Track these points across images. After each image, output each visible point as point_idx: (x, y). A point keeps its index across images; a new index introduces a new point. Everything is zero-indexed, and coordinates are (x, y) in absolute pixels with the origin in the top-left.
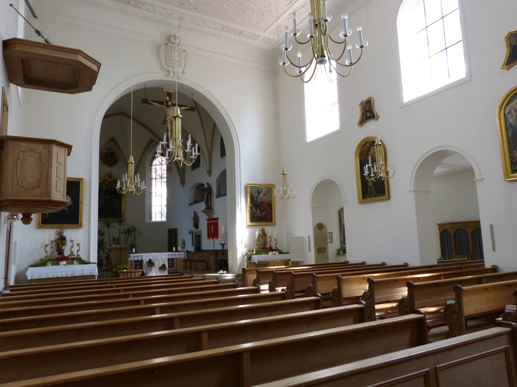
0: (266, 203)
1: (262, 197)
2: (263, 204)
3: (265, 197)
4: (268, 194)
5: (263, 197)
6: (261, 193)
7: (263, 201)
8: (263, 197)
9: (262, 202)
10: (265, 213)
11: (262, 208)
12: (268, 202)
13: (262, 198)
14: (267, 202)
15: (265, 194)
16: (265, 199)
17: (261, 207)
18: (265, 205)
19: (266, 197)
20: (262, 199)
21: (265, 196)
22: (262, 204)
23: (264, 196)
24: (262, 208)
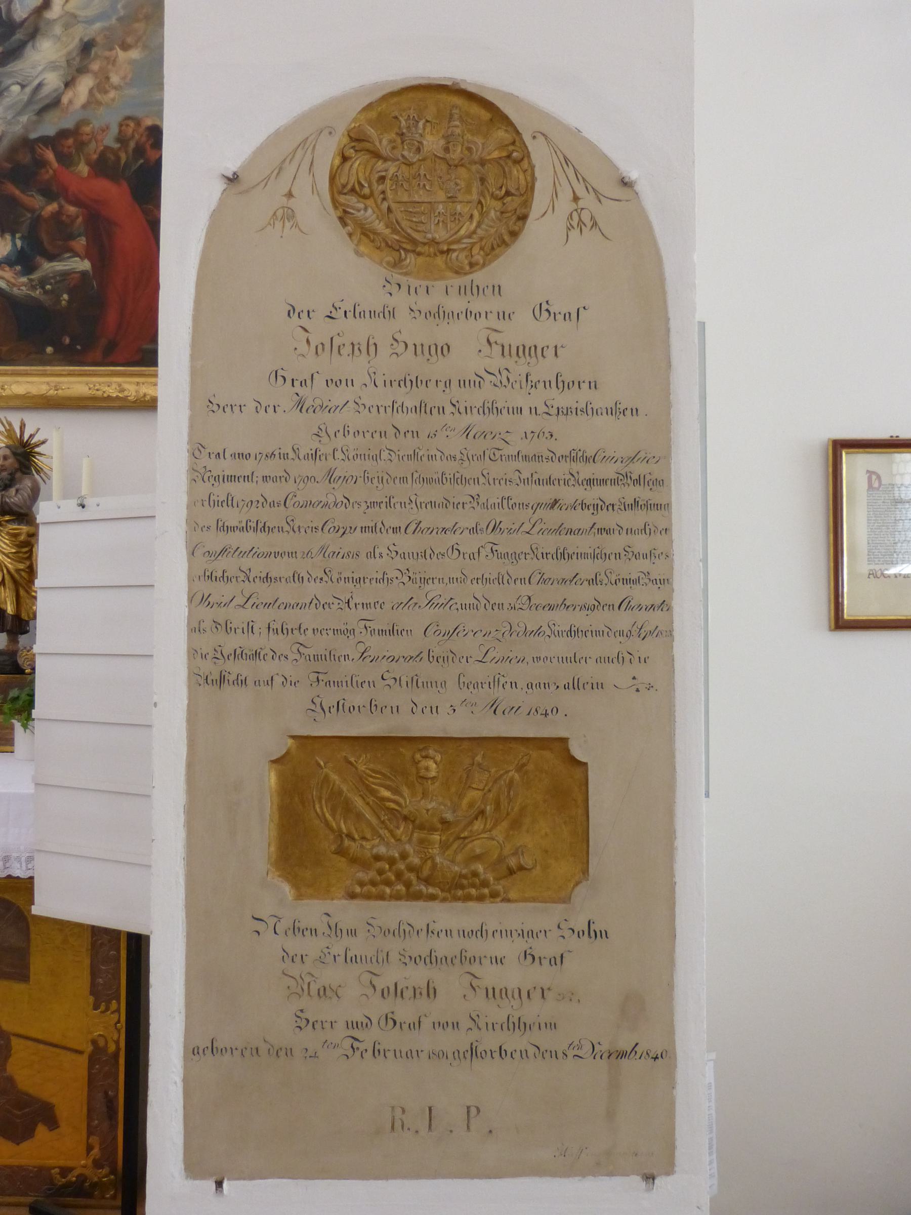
0: (93, 150)
1: (53, 80)
2: (65, 159)
3: (85, 84)
4: (125, 47)
5: (69, 84)
6: (34, 35)
7: (68, 123)
8: (69, 84)
9: (45, 141)
10: (85, 265)
11: (53, 207)
12: (122, 139)
13: (45, 91)
14: (109, 140)
15: (87, 47)
16: (92, 102)
17: (35, 200)
18: (83, 169)
19: (103, 84)
20: (55, 103)
21: (95, 66)
22: (50, 155)
23: (82, 70)
24: (53, 207)
